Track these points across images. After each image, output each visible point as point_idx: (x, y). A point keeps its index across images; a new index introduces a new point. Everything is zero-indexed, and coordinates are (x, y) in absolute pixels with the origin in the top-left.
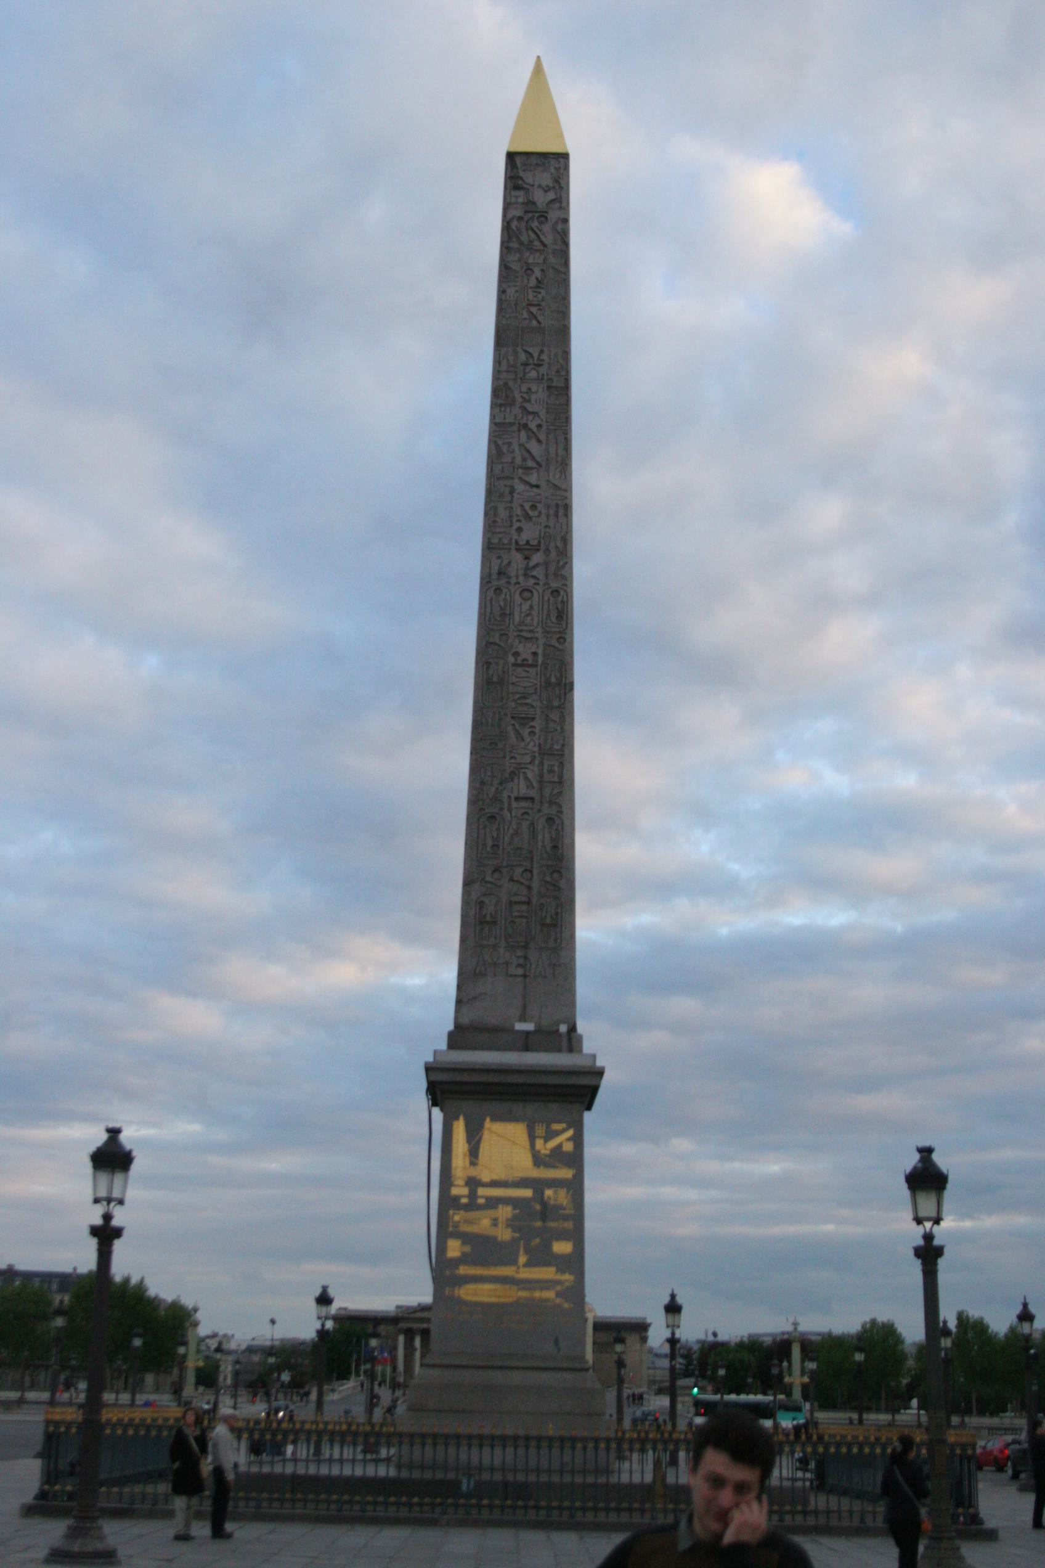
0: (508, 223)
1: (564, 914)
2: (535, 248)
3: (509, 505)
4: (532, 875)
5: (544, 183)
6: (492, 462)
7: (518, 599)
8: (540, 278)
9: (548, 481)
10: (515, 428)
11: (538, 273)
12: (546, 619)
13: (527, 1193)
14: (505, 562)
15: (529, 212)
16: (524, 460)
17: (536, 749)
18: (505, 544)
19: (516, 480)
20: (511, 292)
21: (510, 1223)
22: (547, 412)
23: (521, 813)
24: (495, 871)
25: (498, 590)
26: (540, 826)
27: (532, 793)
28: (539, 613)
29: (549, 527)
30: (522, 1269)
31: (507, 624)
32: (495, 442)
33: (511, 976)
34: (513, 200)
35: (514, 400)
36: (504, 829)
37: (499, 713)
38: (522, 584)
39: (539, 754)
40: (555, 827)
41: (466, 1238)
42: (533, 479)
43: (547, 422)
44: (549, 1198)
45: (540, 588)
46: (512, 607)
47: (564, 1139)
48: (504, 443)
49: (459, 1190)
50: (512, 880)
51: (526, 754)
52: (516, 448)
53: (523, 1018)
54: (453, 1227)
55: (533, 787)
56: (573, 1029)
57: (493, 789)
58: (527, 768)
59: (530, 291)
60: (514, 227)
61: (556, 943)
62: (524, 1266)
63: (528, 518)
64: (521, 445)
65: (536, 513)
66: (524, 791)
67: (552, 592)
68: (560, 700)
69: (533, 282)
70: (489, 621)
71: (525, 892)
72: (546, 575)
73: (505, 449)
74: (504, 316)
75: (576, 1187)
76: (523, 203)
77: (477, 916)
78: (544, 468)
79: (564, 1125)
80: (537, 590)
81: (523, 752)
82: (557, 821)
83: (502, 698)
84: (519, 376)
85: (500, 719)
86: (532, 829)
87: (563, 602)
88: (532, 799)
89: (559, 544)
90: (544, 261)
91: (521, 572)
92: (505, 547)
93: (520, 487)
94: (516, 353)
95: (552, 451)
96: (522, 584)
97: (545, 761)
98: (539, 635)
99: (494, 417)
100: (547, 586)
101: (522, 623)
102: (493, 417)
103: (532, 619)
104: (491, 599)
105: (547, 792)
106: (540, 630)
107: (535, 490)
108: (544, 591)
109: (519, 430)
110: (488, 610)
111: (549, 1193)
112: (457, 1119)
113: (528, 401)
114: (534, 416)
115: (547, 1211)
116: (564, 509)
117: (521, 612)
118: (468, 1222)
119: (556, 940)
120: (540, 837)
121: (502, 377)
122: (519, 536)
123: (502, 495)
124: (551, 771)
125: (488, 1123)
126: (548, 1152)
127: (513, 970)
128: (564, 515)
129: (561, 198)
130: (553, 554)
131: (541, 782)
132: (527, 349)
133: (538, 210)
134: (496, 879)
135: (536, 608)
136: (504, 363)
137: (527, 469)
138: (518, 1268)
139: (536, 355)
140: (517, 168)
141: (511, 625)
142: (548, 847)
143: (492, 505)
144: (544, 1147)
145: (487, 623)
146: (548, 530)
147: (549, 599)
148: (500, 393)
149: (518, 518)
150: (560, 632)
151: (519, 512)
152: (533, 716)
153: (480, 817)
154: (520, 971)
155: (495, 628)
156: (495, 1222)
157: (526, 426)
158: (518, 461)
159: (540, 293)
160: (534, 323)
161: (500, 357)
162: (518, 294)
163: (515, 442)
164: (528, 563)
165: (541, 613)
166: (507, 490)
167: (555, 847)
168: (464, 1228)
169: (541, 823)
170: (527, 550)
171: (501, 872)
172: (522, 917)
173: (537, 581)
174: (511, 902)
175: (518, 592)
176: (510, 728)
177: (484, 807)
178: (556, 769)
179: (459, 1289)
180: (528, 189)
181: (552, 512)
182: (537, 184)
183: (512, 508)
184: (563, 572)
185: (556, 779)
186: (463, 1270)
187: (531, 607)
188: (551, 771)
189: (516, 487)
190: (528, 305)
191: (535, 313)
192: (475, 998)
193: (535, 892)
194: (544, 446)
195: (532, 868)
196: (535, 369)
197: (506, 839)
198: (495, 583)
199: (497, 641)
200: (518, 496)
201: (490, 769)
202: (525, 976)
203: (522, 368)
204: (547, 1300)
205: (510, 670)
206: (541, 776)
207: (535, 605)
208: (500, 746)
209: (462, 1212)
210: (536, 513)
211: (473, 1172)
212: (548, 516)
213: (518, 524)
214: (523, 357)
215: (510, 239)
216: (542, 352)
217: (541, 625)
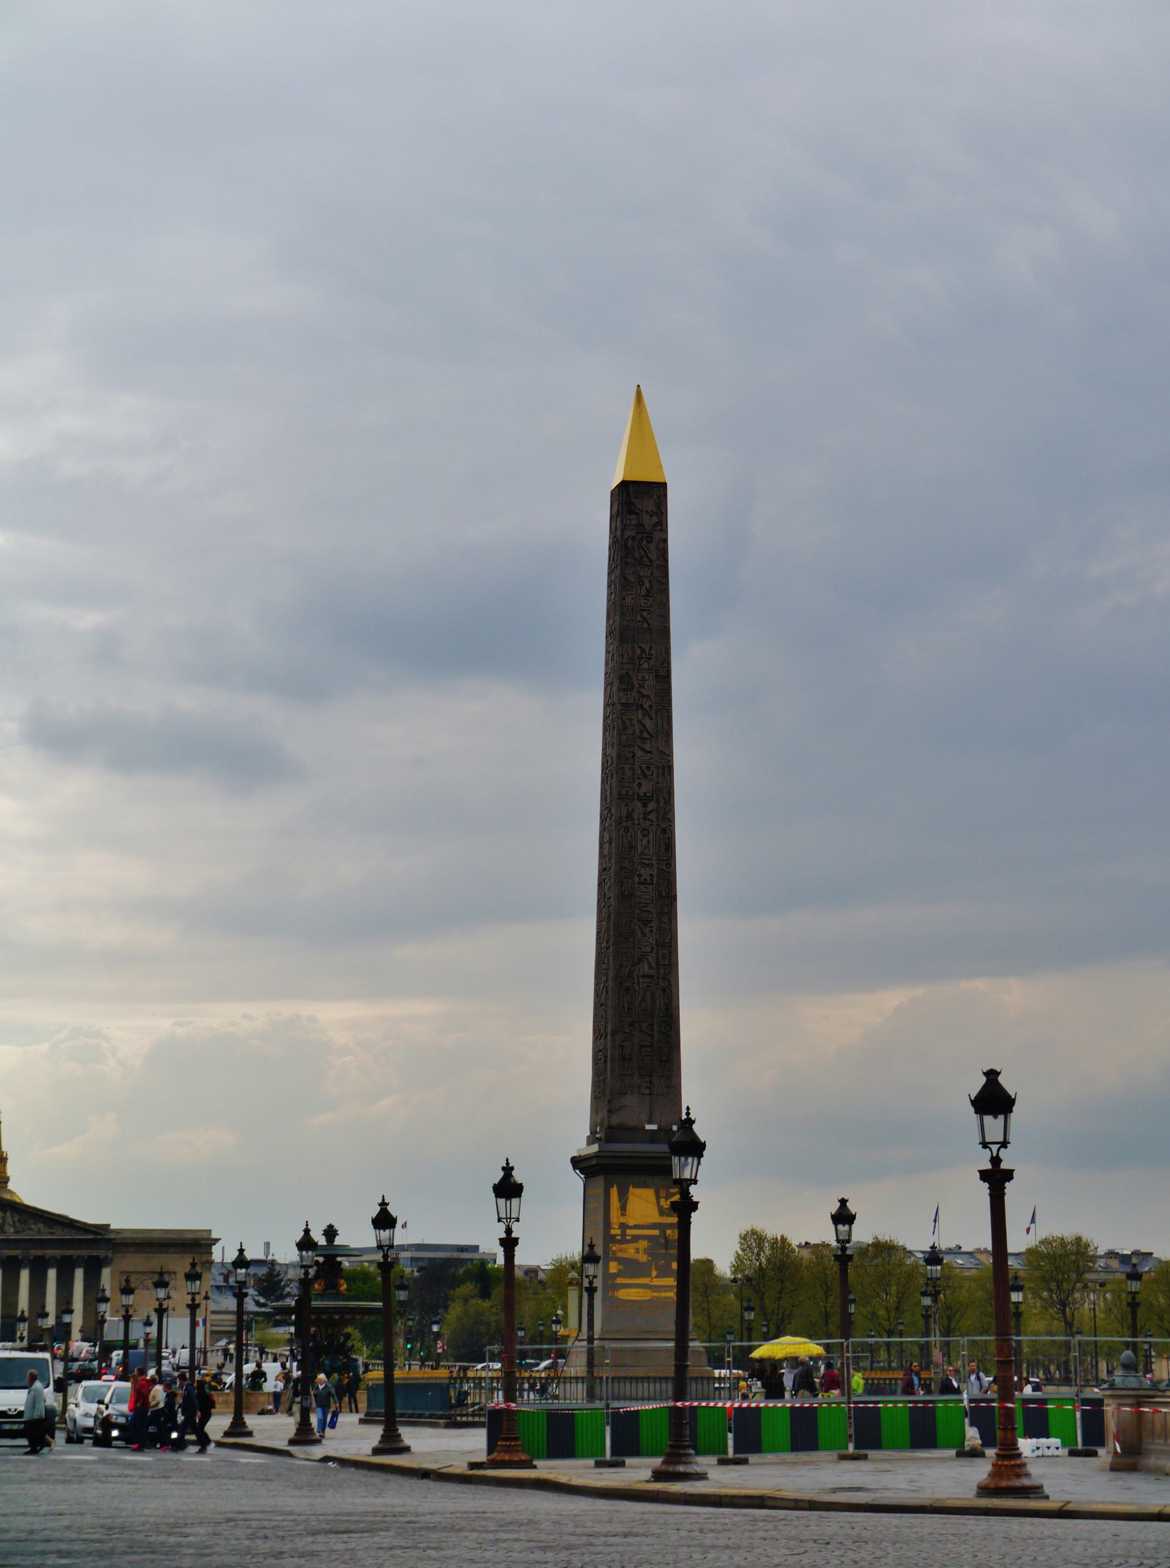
7: (639, 833)
9: (658, 748)
10: (634, 708)
11: (647, 585)
13: (656, 1232)
14: (631, 809)
16: (641, 732)
17: (654, 942)
19: (636, 747)
20: (628, 599)
21: (646, 1251)
22: (656, 696)
24: (630, 1025)
25: (627, 829)
26: (658, 995)
27: (652, 972)
30: (654, 1280)
32: (621, 718)
34: (628, 522)
35: (633, 686)
38: (642, 825)
41: (620, 1261)
42: (647, 747)
45: (654, 828)
48: (627, 719)
50: (641, 1031)
52: (636, 723)
53: (650, 1123)
57: (627, 969)
64: (640, 722)
69: (644, 592)
72: (658, 818)
73: (628, 722)
74: (624, 619)
81: (645, 944)
82: (668, 991)
83: (631, 907)
85: (631, 921)
87: (668, 838)
88: (652, 977)
89: (665, 795)
90: (651, 574)
91: (641, 816)
93: (639, 753)
94: (633, 647)
95: (660, 725)
96: (642, 825)
101: (642, 853)
104: (622, 837)
105: (662, 971)
106: (654, 858)
107: (648, 755)
109: (637, 710)
110: (620, 844)
111: (668, 1232)
113: (643, 687)
120: (658, 1002)
123: (627, 759)
124: (664, 957)
131: (657, 965)
132: (643, 646)
135: (651, 842)
136: (626, 656)
137: (644, 740)
139: (647, 651)
150: (667, 860)
151: (639, 772)
154: (647, 1091)
156: (637, 1251)
158: (637, 732)
166: (631, 755)
167: (667, 1009)
168: (619, 1255)
170: (645, 800)
172: (649, 1056)
176: (637, 927)
179: (617, 1291)
181: (660, 772)
184: (668, 816)
185: (667, 962)
186: (619, 1281)
188: (664, 957)
191: (646, 616)
192: (620, 1109)
193: (655, 1038)
198: (624, 824)
199: (627, 866)
202: (651, 1094)
206: (658, 960)
209: (617, 1245)
210: (650, 773)
211: (623, 1220)
214: (638, 652)
216: (651, 648)
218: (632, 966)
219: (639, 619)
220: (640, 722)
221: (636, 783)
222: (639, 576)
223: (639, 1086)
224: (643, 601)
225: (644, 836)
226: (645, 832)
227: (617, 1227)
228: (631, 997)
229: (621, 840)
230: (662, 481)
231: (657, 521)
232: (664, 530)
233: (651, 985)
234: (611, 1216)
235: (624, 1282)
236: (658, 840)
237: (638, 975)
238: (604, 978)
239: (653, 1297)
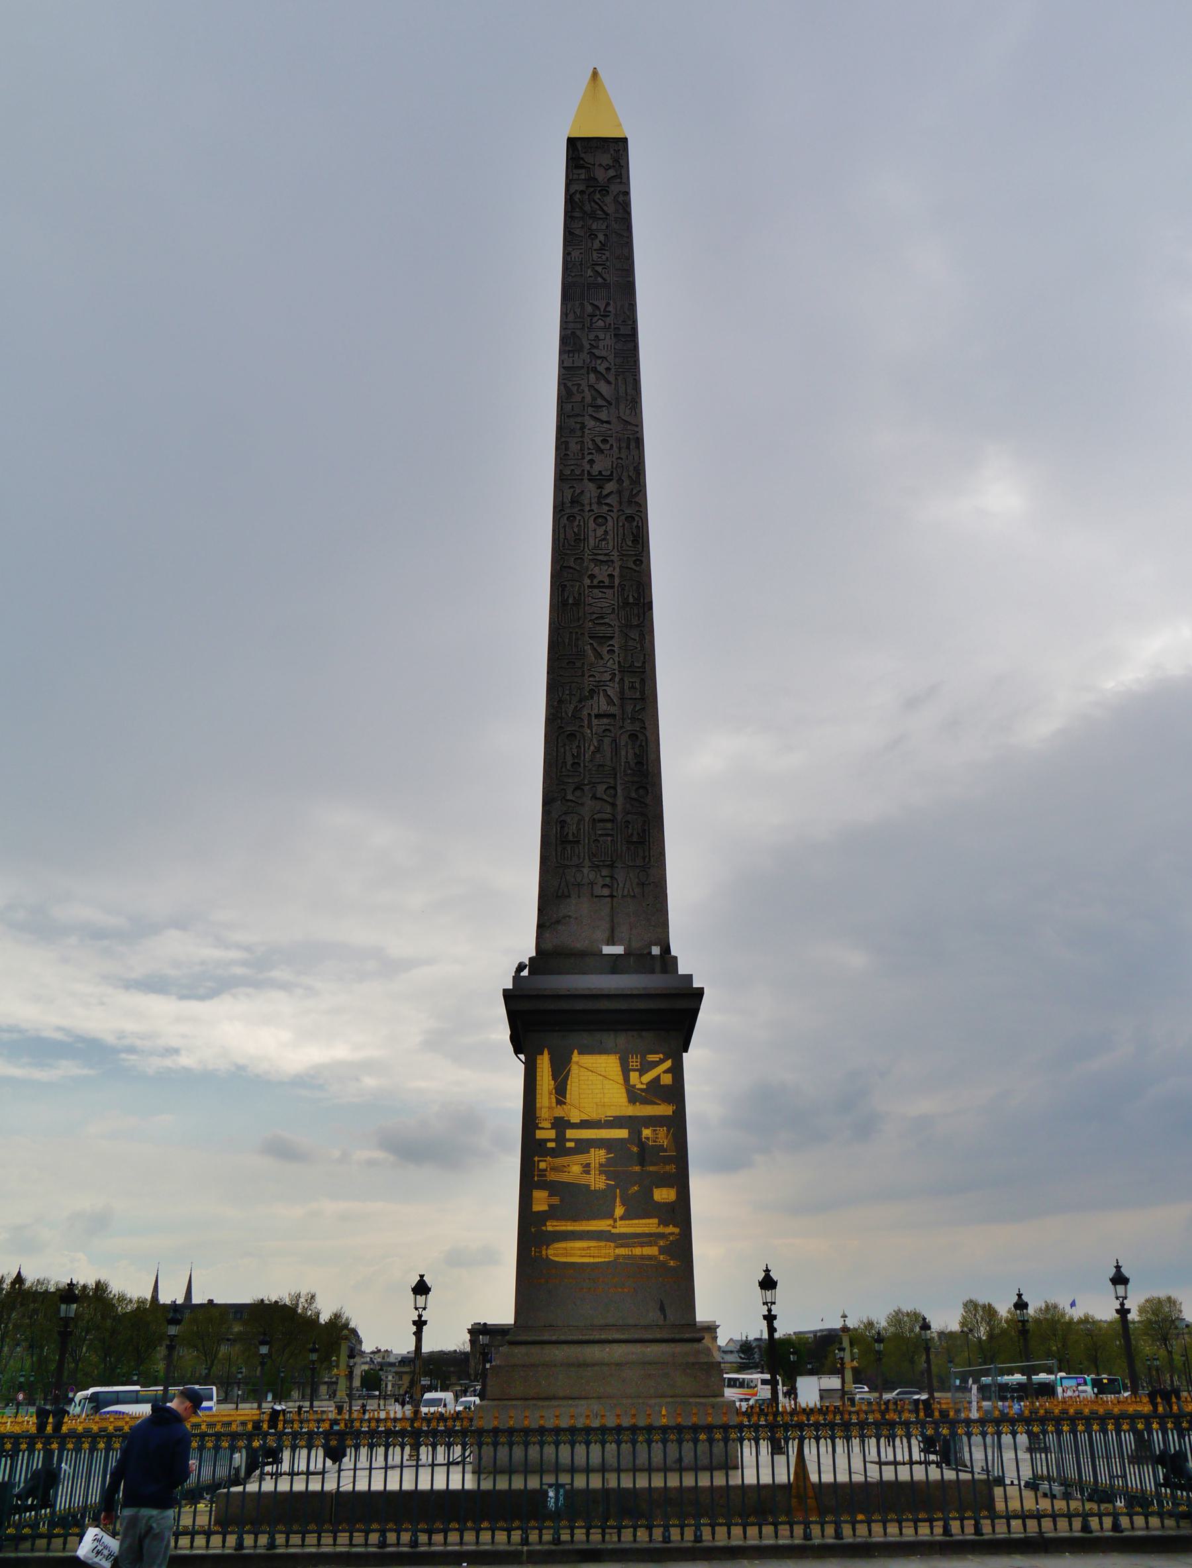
0: (571, 196)
1: (651, 831)
2: (598, 216)
3: (581, 439)
4: (617, 793)
5: (604, 163)
6: (562, 402)
7: (592, 524)
8: (603, 242)
10: (584, 371)
11: (601, 237)
12: (621, 544)
13: (623, 1133)
14: (578, 491)
15: (592, 187)
16: (594, 399)
17: (616, 667)
18: (577, 475)
19: (587, 417)
20: (575, 254)
21: (604, 1169)
23: (602, 730)
24: (575, 789)
26: (623, 743)
27: (612, 710)
28: (614, 538)
29: (622, 459)
30: (619, 1223)
31: (582, 549)
33: (596, 896)
34: (575, 177)
35: (582, 346)
36: (584, 746)
37: (577, 633)
39: (619, 671)
40: (638, 743)
41: (553, 1188)
42: (603, 416)
43: (615, 365)
44: (647, 1138)
45: (614, 515)
46: (586, 533)
47: (661, 1072)
48: (573, 385)
49: (545, 1133)
50: (594, 797)
51: (605, 672)
52: (586, 389)
53: (611, 942)
54: (538, 1175)
55: (615, 705)
56: (666, 949)
57: (572, 706)
58: (607, 686)
59: (594, 253)
60: (577, 200)
61: (644, 862)
62: (622, 1218)
63: (601, 451)
64: (591, 387)
65: (608, 447)
66: (604, 707)
67: (627, 518)
68: (639, 620)
69: (597, 245)
70: (563, 546)
71: (609, 809)
72: (620, 503)
73: (574, 389)
75: (677, 1124)
76: (585, 180)
77: (558, 835)
78: (613, 405)
79: (661, 1056)
80: (610, 516)
83: (579, 620)
84: (586, 325)
85: (577, 639)
86: (614, 745)
87: (637, 527)
88: (613, 716)
90: (607, 227)
91: (594, 500)
92: (576, 477)
93: (591, 423)
94: (582, 305)
95: (622, 390)
96: (596, 511)
97: (626, 679)
98: (615, 558)
99: (563, 361)
100: (622, 513)
101: (596, 547)
102: (561, 362)
103: (608, 543)
104: (565, 527)
105: (629, 709)
106: (615, 553)
107: (605, 425)
108: (618, 518)
109: (588, 373)
110: (562, 536)
111: (646, 1132)
112: (542, 1054)
113: (597, 347)
114: (603, 361)
115: (645, 1153)
117: (596, 538)
118: (554, 1169)
119: (644, 858)
120: (623, 753)
121: (569, 327)
122: (591, 467)
125: (576, 1057)
126: (645, 1087)
127: (598, 891)
128: (636, 448)
129: (621, 174)
130: (626, 483)
132: (596, 303)
133: (599, 185)
134: (577, 797)
135: (611, 533)
138: (615, 1221)
140: (578, 151)
141: (586, 549)
142: (632, 764)
143: (563, 439)
145: (561, 548)
146: (620, 461)
147: (624, 525)
148: (568, 341)
149: (590, 451)
150: (635, 555)
152: (612, 635)
153: (559, 735)
154: (606, 892)
155: (568, 552)
156: (587, 1168)
157: (595, 370)
158: (588, 399)
159: (604, 254)
160: (600, 280)
161: (567, 310)
162: (583, 256)
163: (584, 383)
164: (601, 491)
165: (616, 536)
166: (578, 426)
168: (553, 1177)
169: (624, 739)
170: (600, 480)
171: (583, 790)
172: (607, 835)
173: (610, 509)
174: (594, 819)
175: (592, 518)
177: (563, 725)
178: (637, 686)
179: (548, 1246)
180: (589, 168)
181: (624, 445)
182: (597, 164)
183: (583, 442)
185: (638, 695)
186: (551, 1226)
187: (605, 531)
188: (632, 688)
189: (586, 423)
190: (593, 265)
191: (600, 270)
192: (558, 922)
193: (620, 808)
194: (613, 386)
195: (616, 784)
196: (602, 320)
197: (586, 757)
198: (568, 511)
199: (572, 564)
200: (589, 432)
201: (568, 688)
202: (612, 896)
203: (589, 318)
204: (650, 1258)
205: (586, 592)
206: (622, 692)
207: (610, 530)
208: (578, 664)
209: (548, 1158)
210: (608, 447)
211: (559, 1112)
212: (620, 449)
213: (590, 457)
214: (589, 309)
215: (573, 210)
216: (608, 304)
217: (616, 548)
218: (580, 701)
219: (591, 274)
220: (591, 387)
221: (586, 460)
222: (590, 229)
223: (592, 884)
224: (595, 255)
225: (599, 525)
226: (600, 519)
227: (549, 1126)
228: (579, 747)
229: (562, 531)
231: (615, 174)
232: (627, 183)
233: (611, 728)
234: (538, 1105)
235: (558, 1228)
236: (621, 530)
237: (589, 714)
239: (618, 1257)
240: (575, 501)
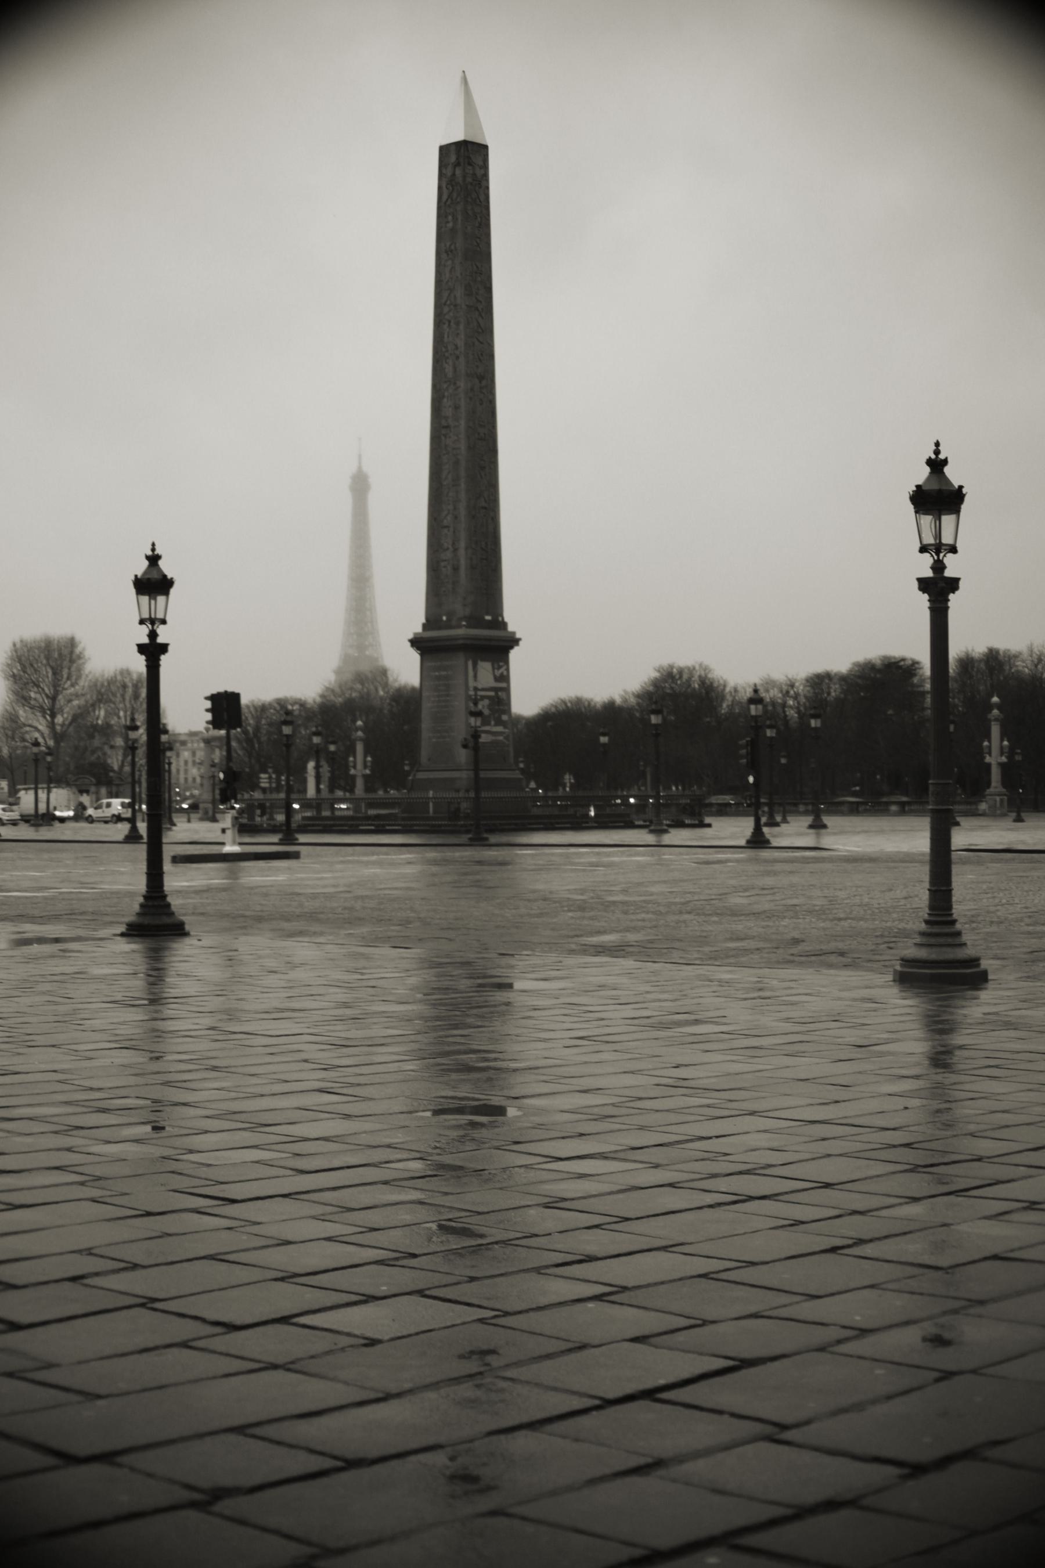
11: (479, 219)
13: (492, 694)
25: (471, 399)
49: (472, 693)
53: (488, 614)
56: (503, 619)
63: (480, 360)
66: (484, 504)
69: (477, 225)
75: (507, 690)
88: (485, 508)
93: (477, 343)
111: (500, 693)
116: (491, 356)
144: (498, 673)
157: (477, 309)
214: (475, 267)
230: (484, 143)
232: (487, 180)
238: (451, 507)
240: (472, 389)
